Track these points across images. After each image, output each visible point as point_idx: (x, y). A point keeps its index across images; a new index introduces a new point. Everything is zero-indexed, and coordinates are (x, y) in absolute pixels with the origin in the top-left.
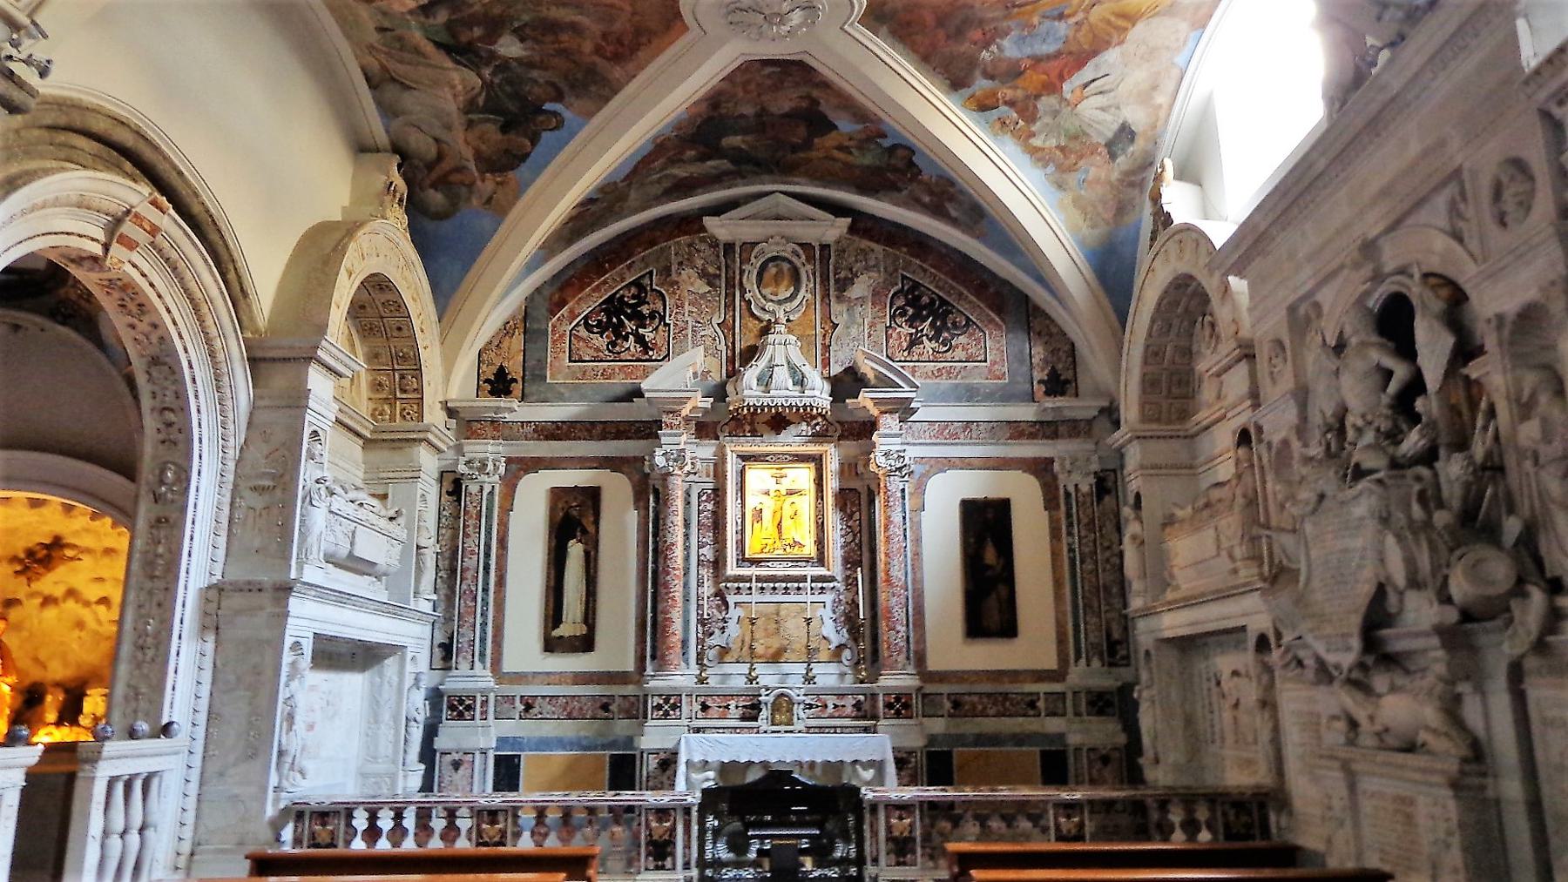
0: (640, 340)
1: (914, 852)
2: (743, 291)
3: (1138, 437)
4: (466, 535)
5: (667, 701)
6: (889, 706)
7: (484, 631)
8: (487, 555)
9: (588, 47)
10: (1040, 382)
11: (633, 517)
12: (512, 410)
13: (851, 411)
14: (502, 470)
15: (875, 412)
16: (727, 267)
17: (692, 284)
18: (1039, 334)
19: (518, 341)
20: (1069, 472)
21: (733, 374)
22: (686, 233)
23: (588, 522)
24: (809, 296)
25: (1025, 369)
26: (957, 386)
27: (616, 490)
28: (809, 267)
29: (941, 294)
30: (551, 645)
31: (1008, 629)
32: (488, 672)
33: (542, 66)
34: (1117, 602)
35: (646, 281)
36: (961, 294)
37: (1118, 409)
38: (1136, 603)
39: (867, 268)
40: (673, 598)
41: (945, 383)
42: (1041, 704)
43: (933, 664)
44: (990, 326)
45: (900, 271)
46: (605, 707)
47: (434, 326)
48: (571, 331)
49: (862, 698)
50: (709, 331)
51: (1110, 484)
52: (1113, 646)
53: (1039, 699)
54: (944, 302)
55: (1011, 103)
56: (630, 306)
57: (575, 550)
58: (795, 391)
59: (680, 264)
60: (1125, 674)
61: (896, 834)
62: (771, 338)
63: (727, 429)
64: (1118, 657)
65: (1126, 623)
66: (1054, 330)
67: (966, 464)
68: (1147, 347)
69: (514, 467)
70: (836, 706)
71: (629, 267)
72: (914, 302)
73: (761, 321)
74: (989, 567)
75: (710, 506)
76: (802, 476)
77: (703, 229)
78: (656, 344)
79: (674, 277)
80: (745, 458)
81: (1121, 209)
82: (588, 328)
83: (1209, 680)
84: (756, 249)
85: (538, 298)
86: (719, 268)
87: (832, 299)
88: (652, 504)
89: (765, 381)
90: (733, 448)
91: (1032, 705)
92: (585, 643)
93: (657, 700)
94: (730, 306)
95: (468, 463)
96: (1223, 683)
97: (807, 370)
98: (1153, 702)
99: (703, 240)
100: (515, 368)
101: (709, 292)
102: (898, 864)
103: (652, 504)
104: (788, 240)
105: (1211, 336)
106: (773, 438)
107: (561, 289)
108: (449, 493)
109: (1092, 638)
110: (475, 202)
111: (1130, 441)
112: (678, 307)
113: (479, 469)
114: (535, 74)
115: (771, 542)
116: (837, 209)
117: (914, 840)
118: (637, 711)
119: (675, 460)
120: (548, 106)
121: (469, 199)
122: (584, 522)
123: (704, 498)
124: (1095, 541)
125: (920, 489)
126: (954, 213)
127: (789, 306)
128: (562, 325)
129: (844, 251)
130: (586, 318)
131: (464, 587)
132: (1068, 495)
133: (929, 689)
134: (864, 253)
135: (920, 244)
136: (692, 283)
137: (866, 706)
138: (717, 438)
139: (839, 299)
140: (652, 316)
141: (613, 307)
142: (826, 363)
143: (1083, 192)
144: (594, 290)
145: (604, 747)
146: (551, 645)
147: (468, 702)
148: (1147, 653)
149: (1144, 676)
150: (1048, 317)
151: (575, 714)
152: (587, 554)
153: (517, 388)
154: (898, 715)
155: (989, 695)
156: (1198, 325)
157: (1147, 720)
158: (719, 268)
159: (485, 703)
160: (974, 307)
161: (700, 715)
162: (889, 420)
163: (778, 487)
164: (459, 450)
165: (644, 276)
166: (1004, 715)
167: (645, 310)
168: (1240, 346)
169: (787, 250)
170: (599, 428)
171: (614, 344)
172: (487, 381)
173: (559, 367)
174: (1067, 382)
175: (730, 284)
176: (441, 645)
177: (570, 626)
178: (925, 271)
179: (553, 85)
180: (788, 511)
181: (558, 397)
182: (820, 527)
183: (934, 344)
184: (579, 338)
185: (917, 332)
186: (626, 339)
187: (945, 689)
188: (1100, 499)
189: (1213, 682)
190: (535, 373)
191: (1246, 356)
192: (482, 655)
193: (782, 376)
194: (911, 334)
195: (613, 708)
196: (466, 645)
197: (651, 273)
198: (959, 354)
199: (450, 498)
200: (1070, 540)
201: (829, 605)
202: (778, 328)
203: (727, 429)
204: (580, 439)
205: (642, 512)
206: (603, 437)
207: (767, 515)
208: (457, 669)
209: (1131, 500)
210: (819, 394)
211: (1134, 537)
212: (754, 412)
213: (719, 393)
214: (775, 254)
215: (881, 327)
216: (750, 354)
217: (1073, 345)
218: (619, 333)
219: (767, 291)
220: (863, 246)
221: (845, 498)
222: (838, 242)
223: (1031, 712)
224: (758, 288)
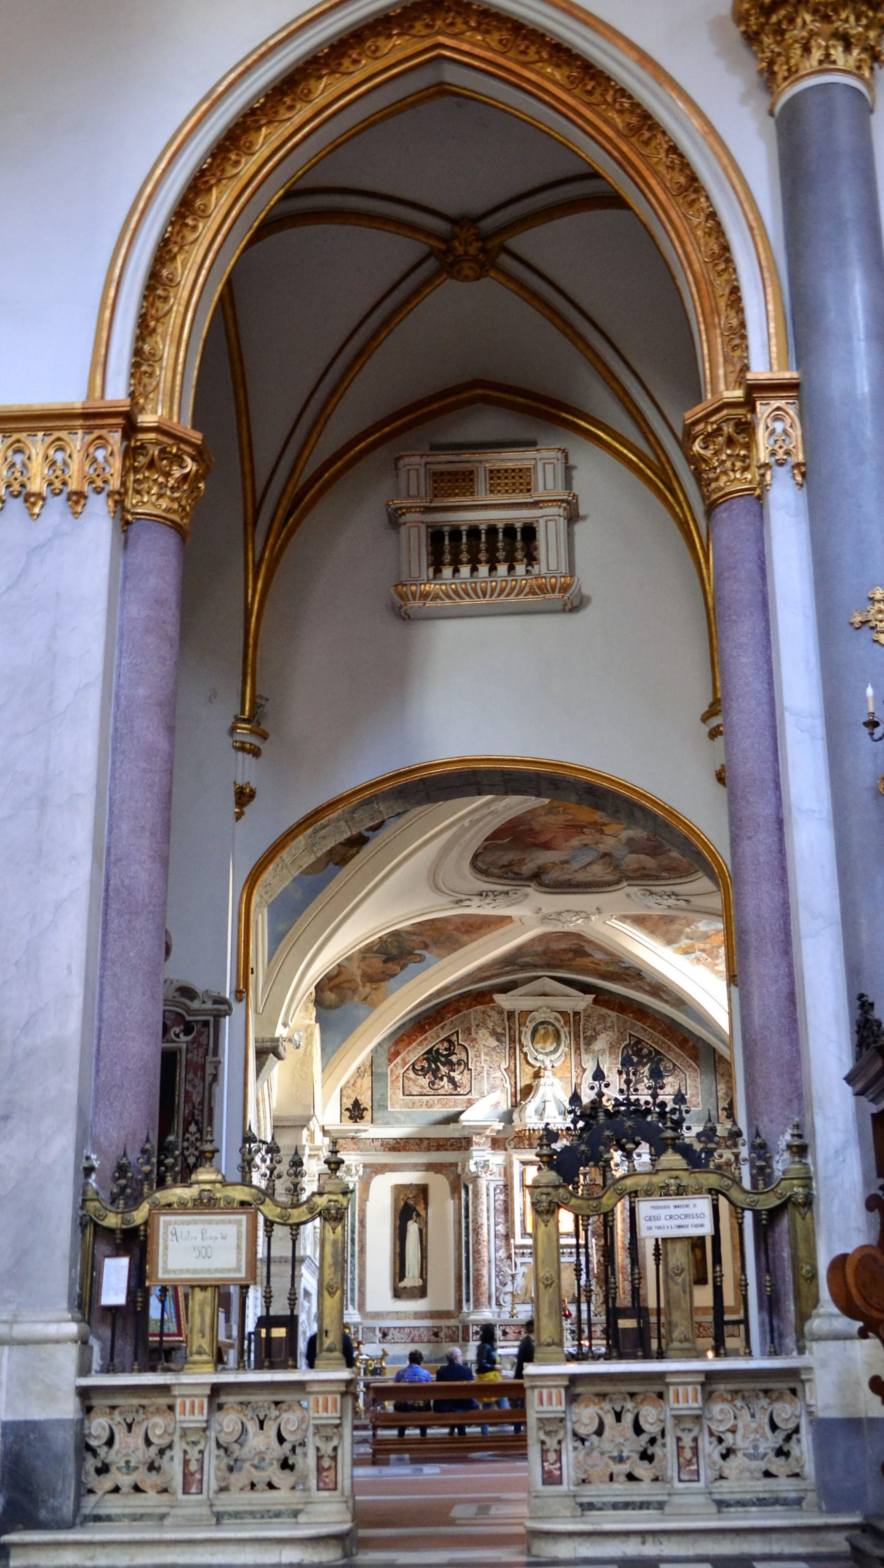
0: (451, 1080)
2: (522, 1046)
9: (451, 927)
10: (724, 1109)
11: (451, 1204)
14: (361, 1173)
16: (510, 1028)
19: (367, 1081)
22: (481, 1004)
23: (420, 1208)
24: (566, 1049)
25: (713, 1100)
27: (439, 1185)
28: (566, 1029)
30: (398, 1294)
32: (356, 1312)
33: (419, 935)
35: (454, 1038)
36: (669, 1047)
46: (436, 1334)
50: (498, 1074)
54: (658, 1053)
55: (703, 951)
56: (443, 1056)
57: (413, 1228)
59: (478, 1025)
62: (542, 1081)
63: (512, 1143)
69: (368, 1170)
71: (442, 1028)
75: (502, 1197)
77: (492, 1001)
79: (473, 1035)
85: (381, 1051)
86: (504, 1029)
87: (582, 1050)
89: (541, 1113)
92: (422, 1292)
93: (476, 1328)
99: (493, 1008)
100: (365, 1101)
107: (396, 1043)
110: (356, 998)
114: (414, 937)
116: (585, 988)
120: (417, 952)
121: (352, 998)
122: (418, 1208)
126: (665, 997)
127: (553, 1057)
128: (397, 1068)
130: (413, 1065)
134: (603, 1017)
135: (641, 1012)
138: (506, 1150)
139: (587, 1051)
140: (459, 1063)
141: (432, 1056)
144: (418, 1045)
146: (398, 1294)
151: (416, 1339)
152: (421, 1231)
153: (367, 1115)
158: (504, 1029)
160: (679, 1056)
161: (502, 1338)
167: (454, 1058)
169: (551, 1017)
170: (426, 1143)
171: (433, 1083)
172: (347, 1109)
173: (396, 1102)
175: (512, 1040)
177: (412, 1279)
178: (645, 1030)
179: (424, 942)
181: (397, 1121)
184: (409, 1079)
186: (442, 1079)
190: (379, 1104)
195: (442, 1334)
197: (457, 1032)
202: (548, 1073)
203: (512, 1143)
206: (428, 1149)
213: (507, 1118)
216: (528, 1091)
219: (538, 1046)
222: (585, 1010)
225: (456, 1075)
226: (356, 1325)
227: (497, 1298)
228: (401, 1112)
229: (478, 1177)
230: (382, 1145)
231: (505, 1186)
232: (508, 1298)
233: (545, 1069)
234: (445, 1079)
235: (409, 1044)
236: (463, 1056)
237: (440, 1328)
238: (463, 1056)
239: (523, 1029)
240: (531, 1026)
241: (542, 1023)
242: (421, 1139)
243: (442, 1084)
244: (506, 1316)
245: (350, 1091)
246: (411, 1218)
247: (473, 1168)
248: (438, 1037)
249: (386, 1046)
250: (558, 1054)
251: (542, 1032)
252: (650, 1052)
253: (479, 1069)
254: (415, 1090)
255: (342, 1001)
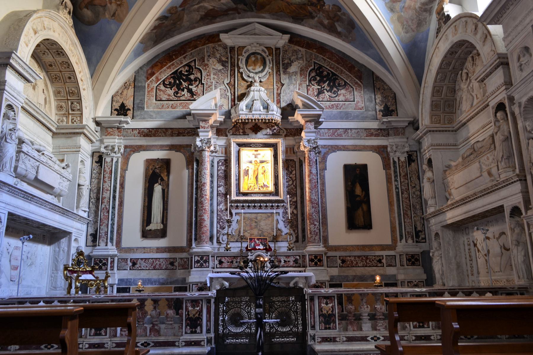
0: (190, 91)
1: (335, 322)
2: (239, 68)
3: (430, 131)
4: (104, 182)
5: (202, 258)
6: (311, 260)
7: (112, 228)
8: (115, 191)
10: (380, 111)
11: (186, 173)
12: (127, 123)
13: (291, 123)
14: (122, 150)
15: (302, 121)
16: (231, 57)
17: (214, 65)
18: (379, 89)
19: (131, 91)
20: (395, 151)
21: (234, 104)
22: (211, 43)
23: (164, 175)
24: (270, 71)
26: (341, 112)
28: (270, 58)
29: (333, 71)
30: (145, 234)
31: (368, 226)
32: (114, 247)
34: (419, 212)
35: (193, 64)
36: (342, 71)
37: (418, 120)
38: (431, 210)
39: (297, 59)
40: (205, 209)
41: (335, 111)
42: (384, 261)
43: (332, 242)
44: (356, 85)
45: (313, 60)
46: (172, 264)
47: (89, 80)
48: (156, 87)
49: (298, 257)
51: (414, 158)
52: (417, 233)
53: (383, 258)
54: (334, 74)
57: (158, 189)
58: (263, 111)
59: (209, 56)
60: (424, 247)
61: (325, 312)
62: (252, 88)
64: (420, 238)
65: (424, 220)
66: (386, 87)
67: (345, 148)
68: (434, 87)
69: (128, 150)
70: (285, 261)
71: (185, 58)
72: (320, 74)
73: (247, 82)
74: (358, 196)
75: (223, 168)
76: (267, 154)
77: (220, 40)
78: (197, 93)
79: (206, 62)
80: (240, 145)
81: (420, 23)
82: (165, 85)
83: (469, 245)
84: (245, 49)
85: (141, 72)
86: (227, 58)
87: (281, 72)
88: (195, 166)
89: (250, 107)
90: (234, 141)
91: (380, 261)
92: (162, 233)
94: (233, 75)
95: (105, 147)
96: (478, 245)
97: (269, 102)
98: (441, 257)
99: (220, 45)
100: (129, 104)
101: (223, 69)
102: (326, 328)
103: (195, 166)
104: (261, 45)
105: (467, 79)
106: (254, 135)
107: (152, 67)
108: (96, 162)
109: (408, 230)
111: (425, 134)
112: (208, 76)
113: (111, 150)
115: (252, 185)
116: (283, 31)
117: (335, 316)
118: (187, 265)
119: (206, 143)
122: (162, 175)
123: (220, 164)
124: (408, 184)
125: (324, 160)
126: (339, 29)
127: (260, 75)
128: (153, 84)
129: (286, 51)
130: (164, 81)
131: (103, 206)
132: (394, 162)
133: (330, 254)
136: (215, 65)
137: (300, 261)
138: (227, 136)
139: (285, 72)
140: (196, 79)
141: (177, 76)
142: (279, 102)
143: (402, 14)
144: (168, 68)
145: (171, 283)
146: (145, 234)
147: (104, 262)
148: (437, 234)
149: (435, 244)
150: (383, 81)
151: (157, 267)
152: (163, 190)
153: (130, 113)
154: (316, 265)
155: (359, 257)
156: (459, 76)
157: (437, 267)
159: (112, 262)
160: (349, 77)
161: (218, 266)
162: (310, 125)
163: (256, 159)
164: (101, 141)
165: (192, 61)
166: (366, 266)
167: (192, 77)
168: (499, 58)
169: (259, 49)
170: (170, 131)
171: (177, 93)
172: (116, 110)
174: (393, 111)
175: (233, 65)
176: (91, 235)
177: (156, 224)
178: (325, 60)
180: (260, 171)
181: (151, 118)
182: (276, 177)
183: (329, 94)
184: (160, 90)
185: (322, 88)
186: (183, 90)
187: (338, 254)
188: (410, 164)
189: (472, 244)
190: (139, 106)
191: (502, 64)
192: (112, 239)
193: (258, 105)
194: (319, 89)
195: (176, 264)
196: (103, 234)
197: (195, 60)
198: (341, 98)
199: (97, 165)
200: (396, 183)
201: (281, 214)
202: (257, 84)
204: (160, 136)
205: (191, 170)
206: (172, 135)
207: (251, 173)
208: (99, 246)
209: (426, 162)
210: (276, 114)
211: (429, 179)
212: (245, 123)
213: (228, 115)
214: (254, 51)
215: (304, 85)
216: (242, 97)
217: (395, 94)
218: (179, 87)
219: (250, 68)
220: (295, 49)
221: (287, 164)
222: (283, 47)
223: (380, 265)
224: (246, 66)
225: (193, 88)
226: (113, 257)
227: (218, 238)
228: (154, 112)
229: (203, 150)
230: (139, 133)
231: (226, 160)
232: (225, 237)
233: (255, 81)
234: (185, 90)
235: (162, 68)
236: (199, 75)
237: (175, 259)
238: (199, 75)
239: (240, 57)
240: (246, 55)
241: (253, 54)
242: (167, 129)
243: (183, 93)
244: (222, 250)
245: (118, 98)
246: (157, 182)
247: (198, 143)
248: (182, 63)
249: (145, 69)
250: (264, 73)
251: (253, 59)
252: (328, 73)
253: (209, 84)
254: (164, 97)
255: (97, 16)
